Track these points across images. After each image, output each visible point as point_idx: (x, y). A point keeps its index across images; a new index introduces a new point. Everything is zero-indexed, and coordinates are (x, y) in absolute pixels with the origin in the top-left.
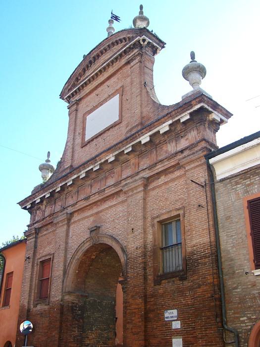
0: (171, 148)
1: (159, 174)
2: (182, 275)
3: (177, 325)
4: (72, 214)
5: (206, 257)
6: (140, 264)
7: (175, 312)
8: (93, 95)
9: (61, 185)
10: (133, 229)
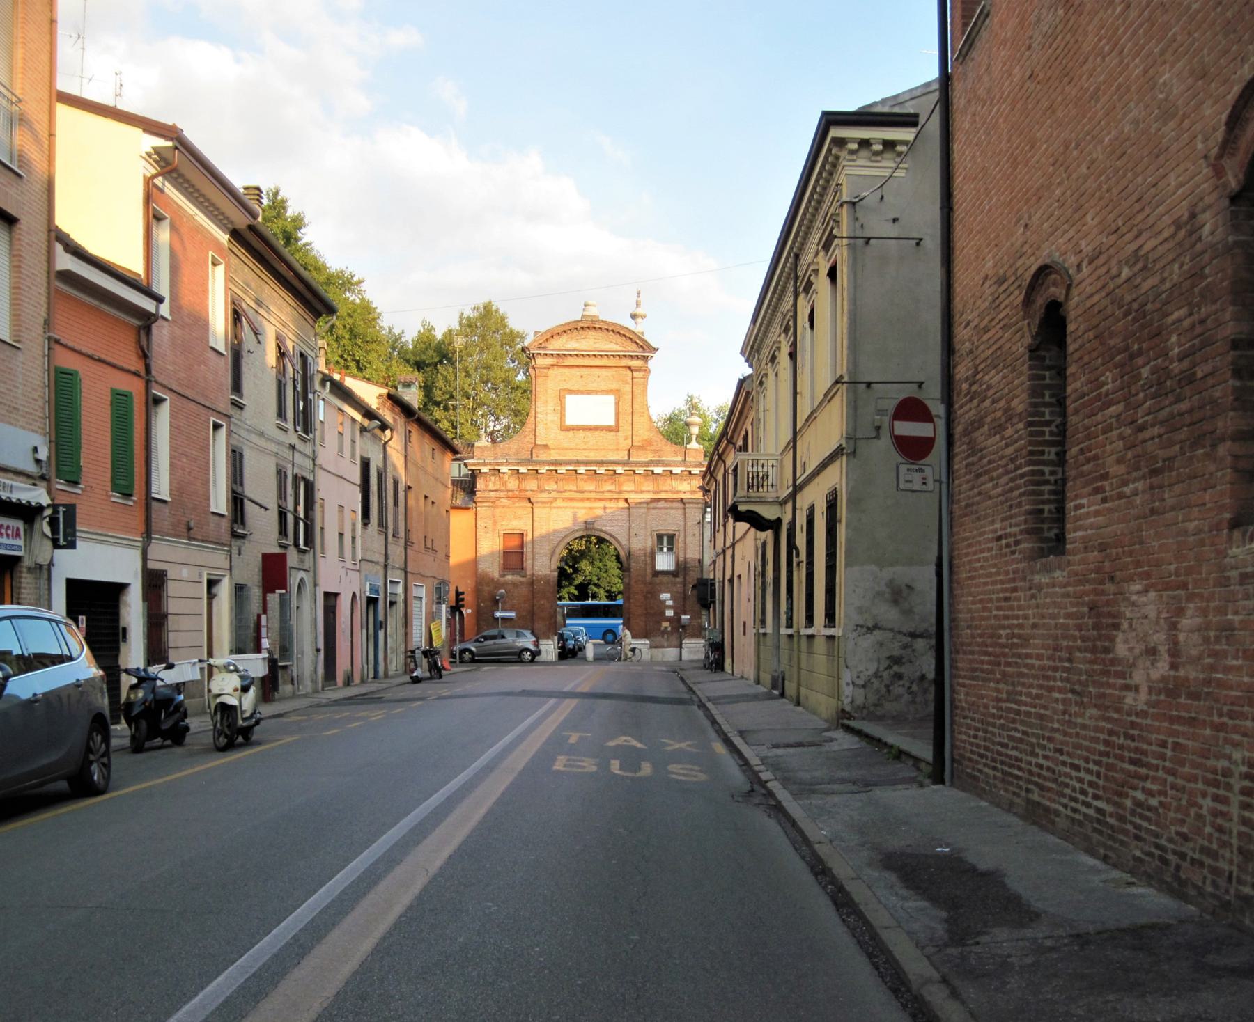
3: (670, 603)
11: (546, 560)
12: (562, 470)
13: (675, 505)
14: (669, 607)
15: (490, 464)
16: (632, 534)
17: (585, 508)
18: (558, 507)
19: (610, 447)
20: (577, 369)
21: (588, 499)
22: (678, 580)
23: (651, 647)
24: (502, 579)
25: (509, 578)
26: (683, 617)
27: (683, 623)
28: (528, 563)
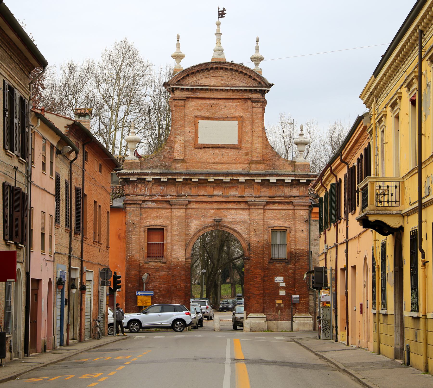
0: (287, 191)
1: (274, 203)
2: (287, 261)
3: (283, 284)
4: (189, 202)
5: (304, 256)
6: (260, 251)
7: (282, 279)
8: (208, 102)
9: (184, 177)
10: (255, 230)
11: (182, 250)
12: (195, 179)
13: (287, 206)
14: (282, 288)
15: (138, 174)
16: (252, 230)
17: (213, 209)
18: (192, 209)
19: (234, 161)
20: (208, 101)
21: (216, 202)
22: (289, 266)
23: (267, 320)
24: (146, 265)
25: (152, 264)
26: (294, 296)
27: (294, 302)
28: (167, 253)
